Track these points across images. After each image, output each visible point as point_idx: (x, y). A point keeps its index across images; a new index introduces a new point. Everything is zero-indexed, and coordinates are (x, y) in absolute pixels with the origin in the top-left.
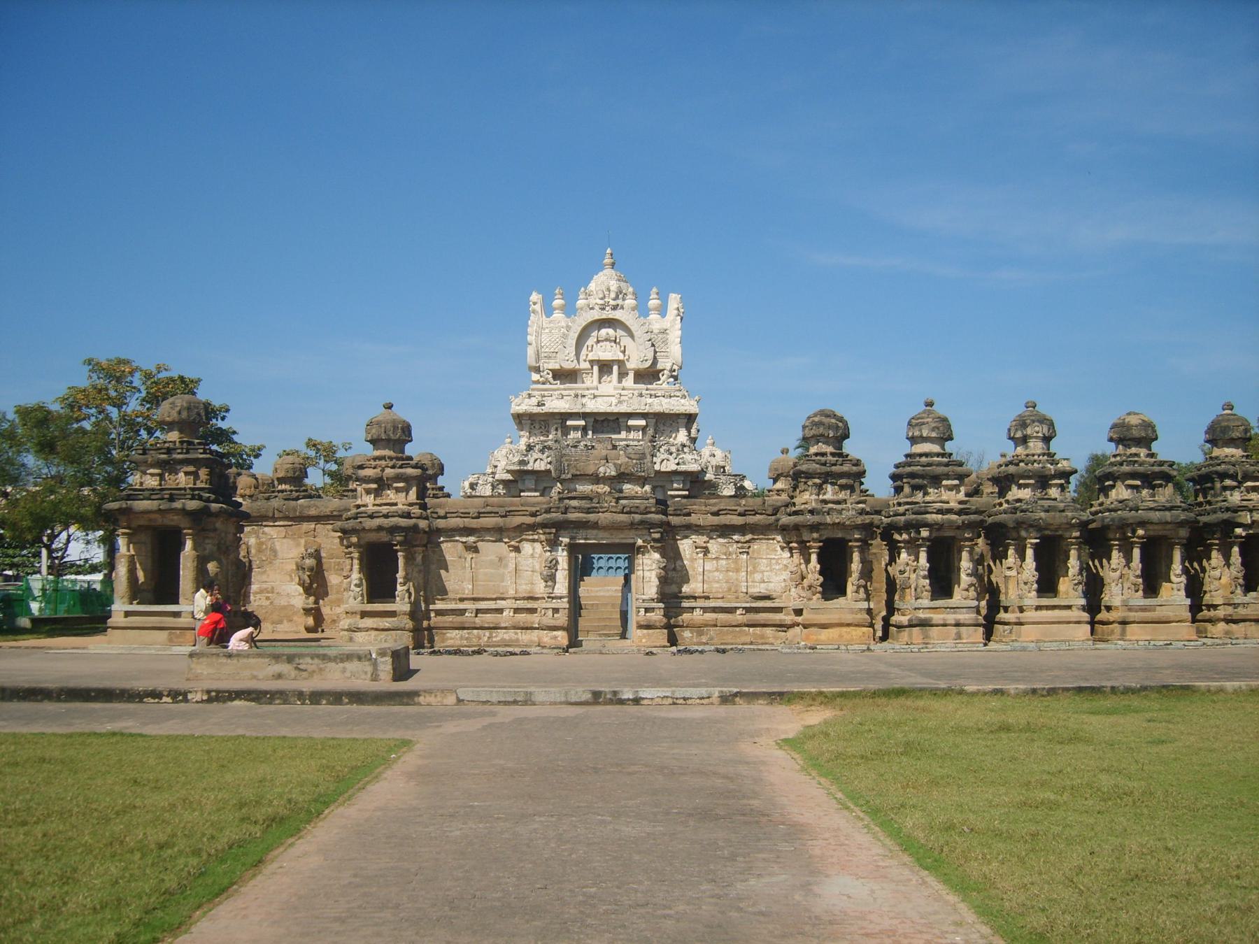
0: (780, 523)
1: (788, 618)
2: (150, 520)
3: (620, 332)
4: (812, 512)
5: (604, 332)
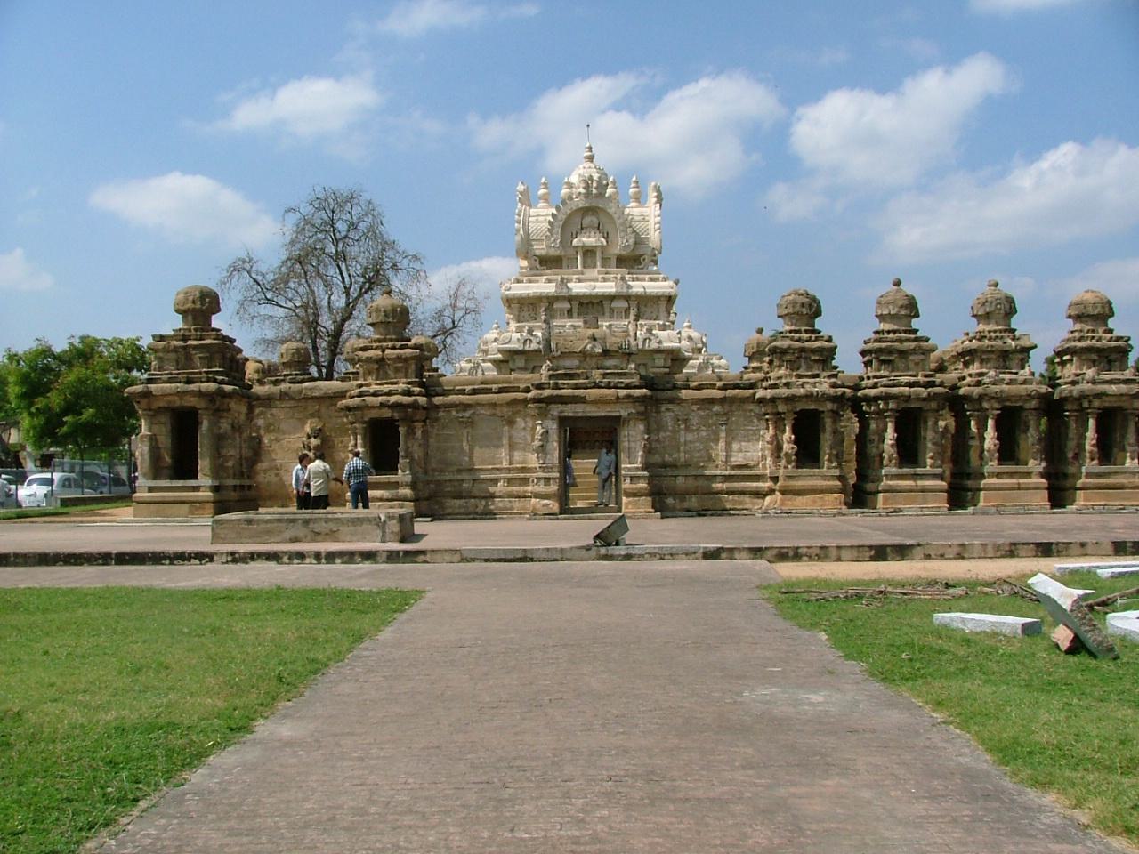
0: (757, 396)
1: (767, 485)
2: (170, 402)
4: (787, 385)
5: (588, 220)
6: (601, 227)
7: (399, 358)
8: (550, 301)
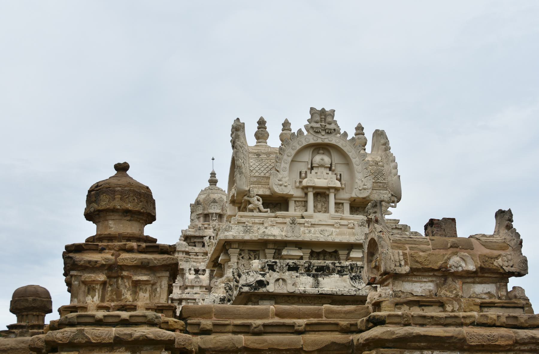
3: (336, 158)
5: (318, 159)
6: (333, 168)
7: (144, 267)
8: (279, 245)
